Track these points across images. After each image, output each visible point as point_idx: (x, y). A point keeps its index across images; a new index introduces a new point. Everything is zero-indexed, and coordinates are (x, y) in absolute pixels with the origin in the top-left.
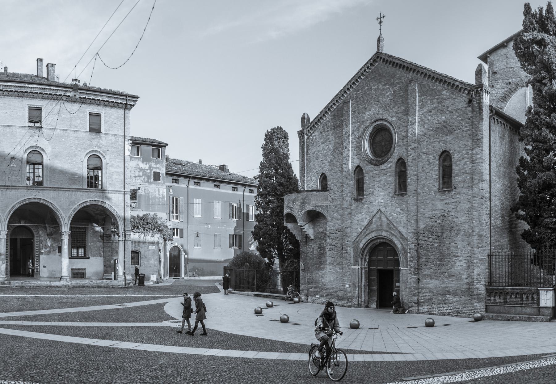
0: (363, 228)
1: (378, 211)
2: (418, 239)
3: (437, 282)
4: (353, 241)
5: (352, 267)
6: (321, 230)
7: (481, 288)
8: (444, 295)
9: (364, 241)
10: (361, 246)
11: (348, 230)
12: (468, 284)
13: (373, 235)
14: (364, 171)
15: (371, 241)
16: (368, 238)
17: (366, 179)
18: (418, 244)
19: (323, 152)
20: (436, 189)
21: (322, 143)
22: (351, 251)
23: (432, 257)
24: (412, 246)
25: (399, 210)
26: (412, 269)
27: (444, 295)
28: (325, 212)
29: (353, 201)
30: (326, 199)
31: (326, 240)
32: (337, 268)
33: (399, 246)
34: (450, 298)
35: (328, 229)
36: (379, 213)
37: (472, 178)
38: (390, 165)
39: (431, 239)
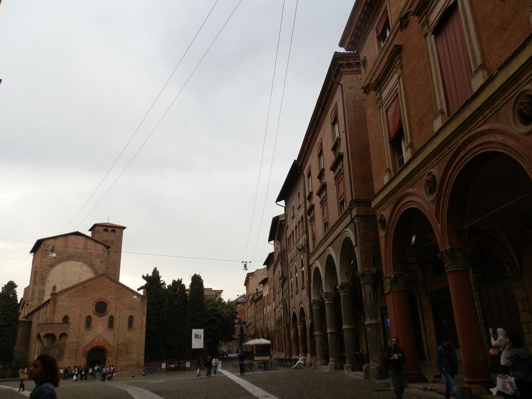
0: (90, 342)
1: (98, 336)
2: (118, 346)
3: (125, 363)
4: (83, 347)
5: (82, 359)
6: (62, 342)
7: (143, 363)
8: (127, 367)
9: (90, 348)
10: (88, 350)
11: (81, 343)
12: (137, 362)
13: (95, 345)
14: (92, 318)
15: (93, 347)
16: (92, 346)
17: (93, 322)
18: (118, 349)
19: (67, 305)
20: (127, 329)
21: (67, 302)
22: (81, 351)
23: (123, 354)
24: (115, 350)
25: (109, 335)
26: (115, 359)
27: (127, 367)
28: (67, 334)
29: (85, 330)
30: (68, 327)
31: (65, 347)
32: (72, 360)
33: (108, 349)
34: (130, 368)
35: (67, 341)
36: (99, 336)
37: (141, 326)
38: (106, 318)
39: (123, 347)
